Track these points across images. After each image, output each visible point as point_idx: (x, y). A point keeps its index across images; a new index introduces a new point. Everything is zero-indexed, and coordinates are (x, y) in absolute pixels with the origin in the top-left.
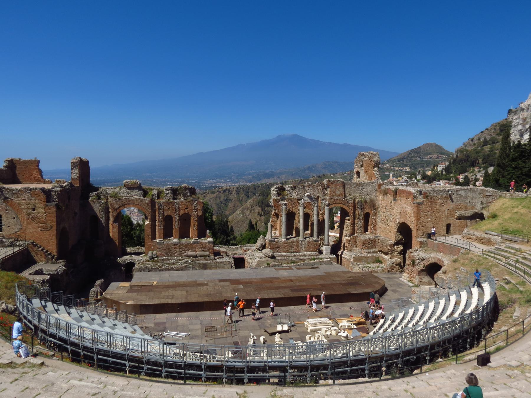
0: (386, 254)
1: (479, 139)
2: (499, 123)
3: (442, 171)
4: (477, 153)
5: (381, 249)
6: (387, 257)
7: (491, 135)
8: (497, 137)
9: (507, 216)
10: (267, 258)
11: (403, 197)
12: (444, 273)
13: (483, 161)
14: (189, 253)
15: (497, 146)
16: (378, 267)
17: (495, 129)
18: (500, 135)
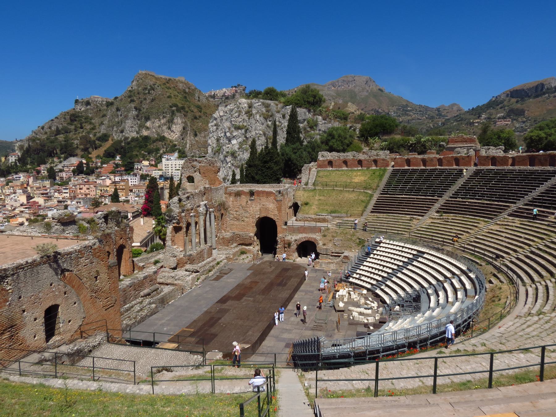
0: (250, 245)
1: (50, 128)
2: (68, 113)
3: (15, 162)
4: (51, 142)
5: (241, 242)
6: (251, 247)
7: (62, 124)
8: (69, 127)
9: (316, 202)
10: (194, 275)
11: (263, 196)
12: (324, 245)
13: (61, 151)
14: (146, 291)
15: (71, 136)
16: (247, 257)
17: (65, 118)
18: (72, 125)
